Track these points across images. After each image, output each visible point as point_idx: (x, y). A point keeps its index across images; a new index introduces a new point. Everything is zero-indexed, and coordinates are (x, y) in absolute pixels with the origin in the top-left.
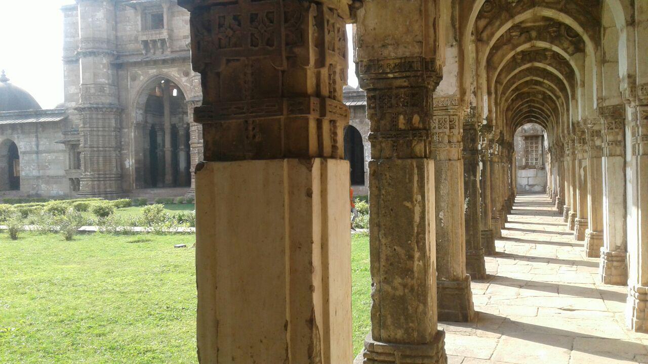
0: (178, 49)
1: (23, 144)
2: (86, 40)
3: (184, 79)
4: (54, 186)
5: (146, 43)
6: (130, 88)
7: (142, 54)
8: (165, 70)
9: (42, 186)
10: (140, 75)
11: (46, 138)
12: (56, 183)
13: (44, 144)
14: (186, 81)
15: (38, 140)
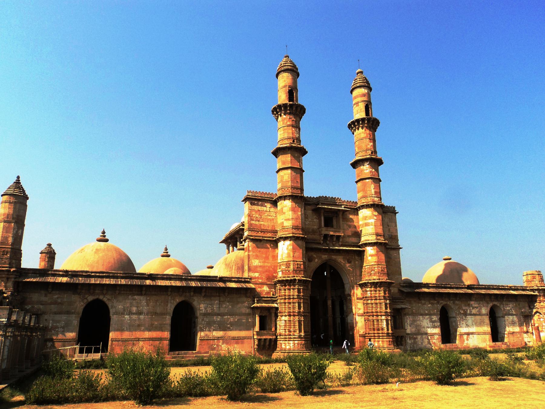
0: (347, 244)
1: (202, 306)
2: (295, 227)
3: (348, 265)
4: (236, 346)
5: (326, 236)
6: (308, 267)
7: (320, 243)
8: (334, 257)
9: (223, 346)
10: (315, 258)
11: (228, 302)
12: (237, 343)
13: (227, 306)
14: (349, 267)
15: (220, 304)
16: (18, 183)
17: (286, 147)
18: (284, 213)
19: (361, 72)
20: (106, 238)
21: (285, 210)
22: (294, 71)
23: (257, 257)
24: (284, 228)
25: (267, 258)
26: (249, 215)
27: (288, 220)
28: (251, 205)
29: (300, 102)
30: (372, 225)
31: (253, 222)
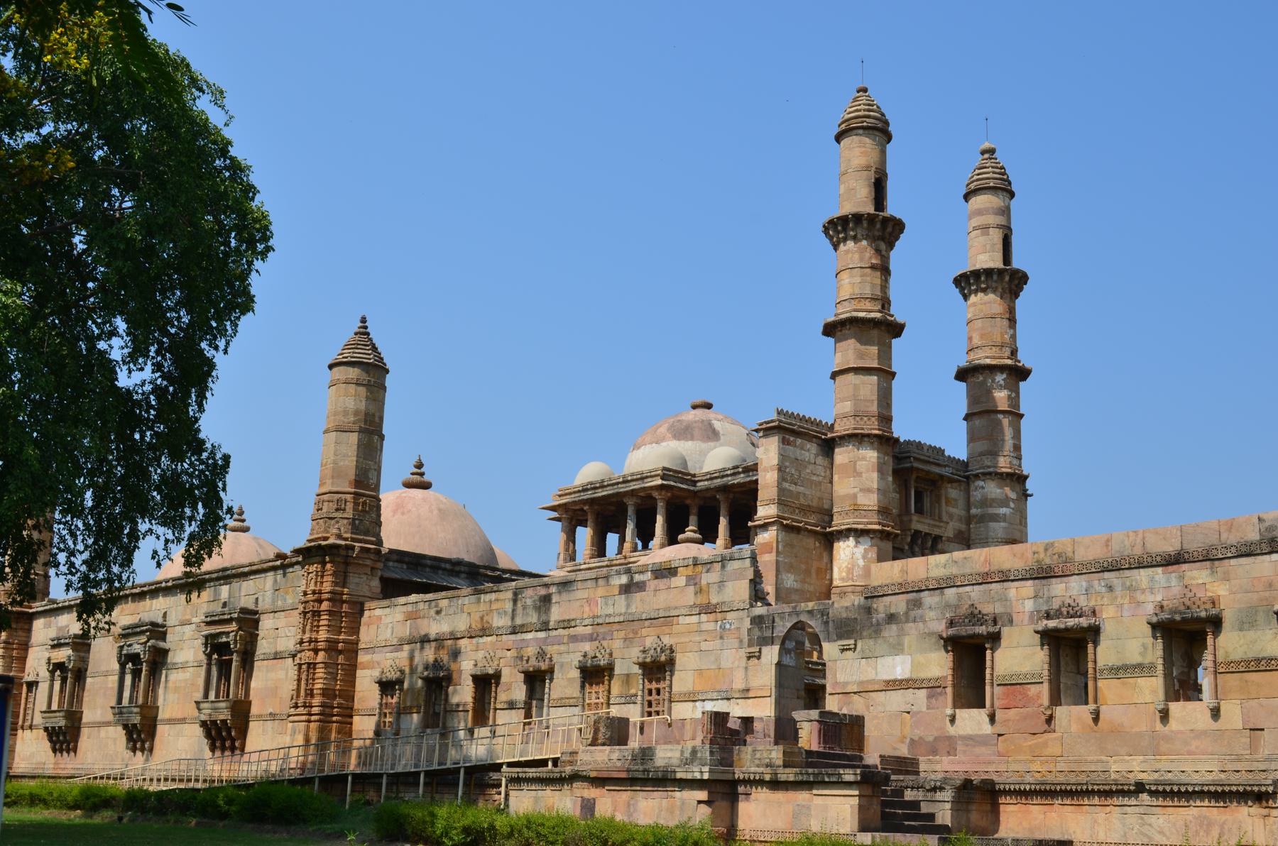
16: (364, 332)
17: (872, 320)
18: (859, 474)
19: (992, 151)
20: (426, 478)
21: (861, 465)
22: (880, 130)
23: (791, 568)
24: (856, 509)
25: (808, 572)
26: (780, 469)
27: (869, 490)
28: (784, 442)
29: (893, 208)
30: (1005, 521)
31: (786, 485)
